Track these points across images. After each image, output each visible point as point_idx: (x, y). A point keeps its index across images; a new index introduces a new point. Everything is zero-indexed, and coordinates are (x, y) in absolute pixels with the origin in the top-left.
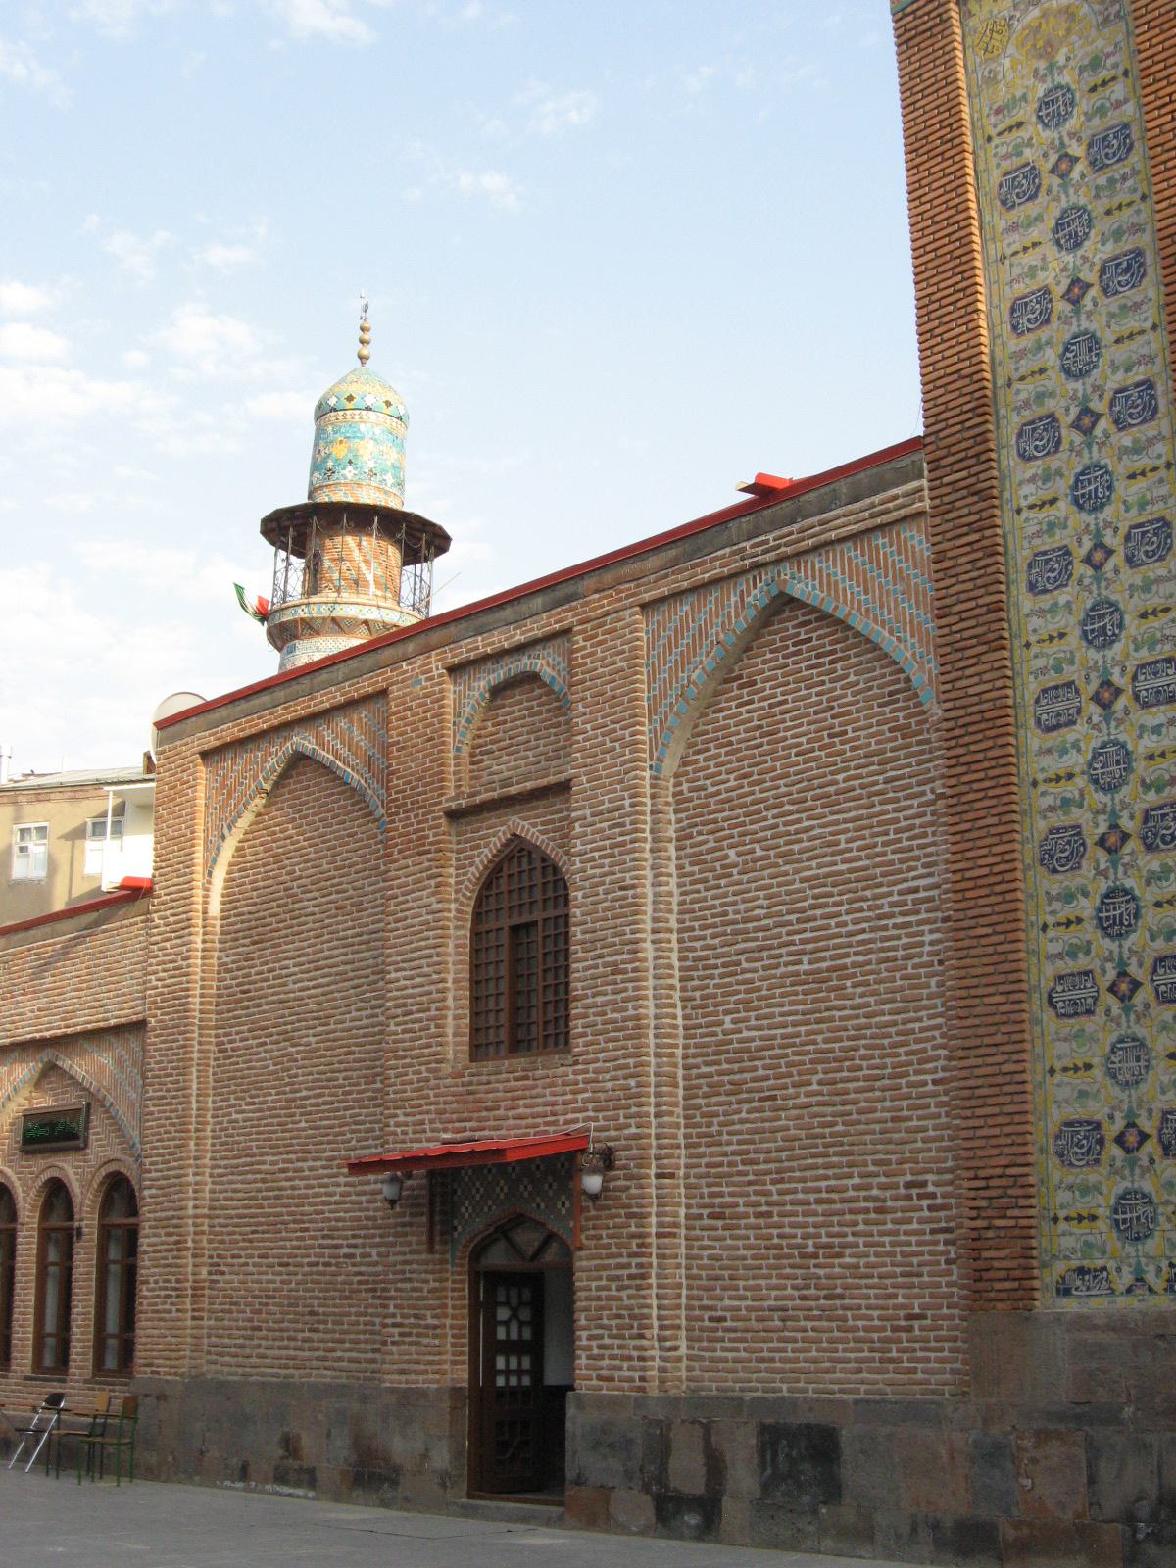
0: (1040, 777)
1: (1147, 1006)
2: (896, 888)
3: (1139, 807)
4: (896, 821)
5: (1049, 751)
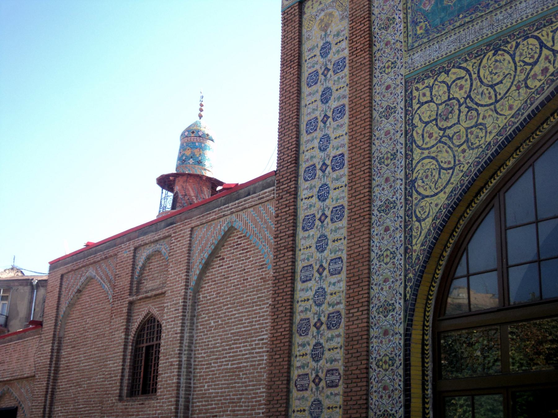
0: (300, 300)
1: (323, 388)
2: (257, 338)
3: (327, 313)
4: (259, 313)
5: (303, 290)
